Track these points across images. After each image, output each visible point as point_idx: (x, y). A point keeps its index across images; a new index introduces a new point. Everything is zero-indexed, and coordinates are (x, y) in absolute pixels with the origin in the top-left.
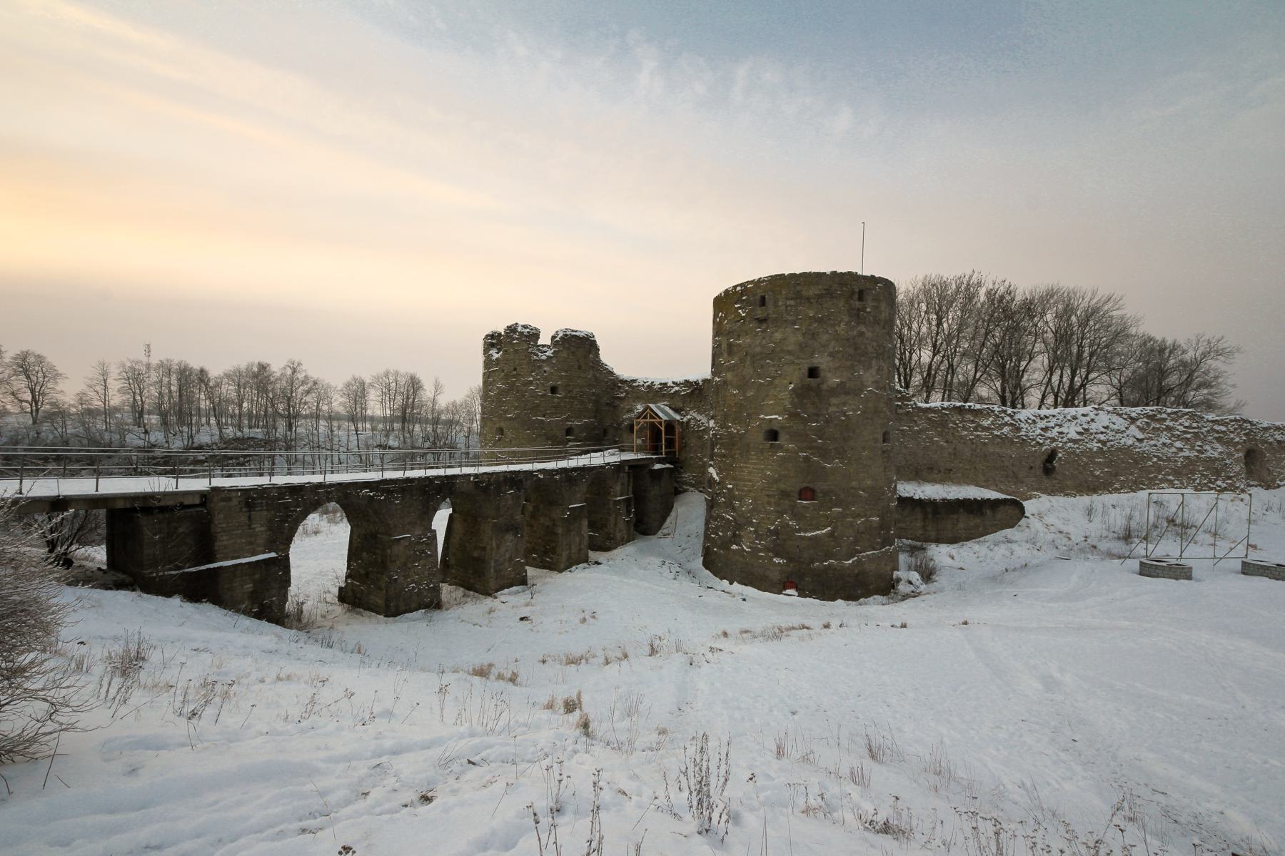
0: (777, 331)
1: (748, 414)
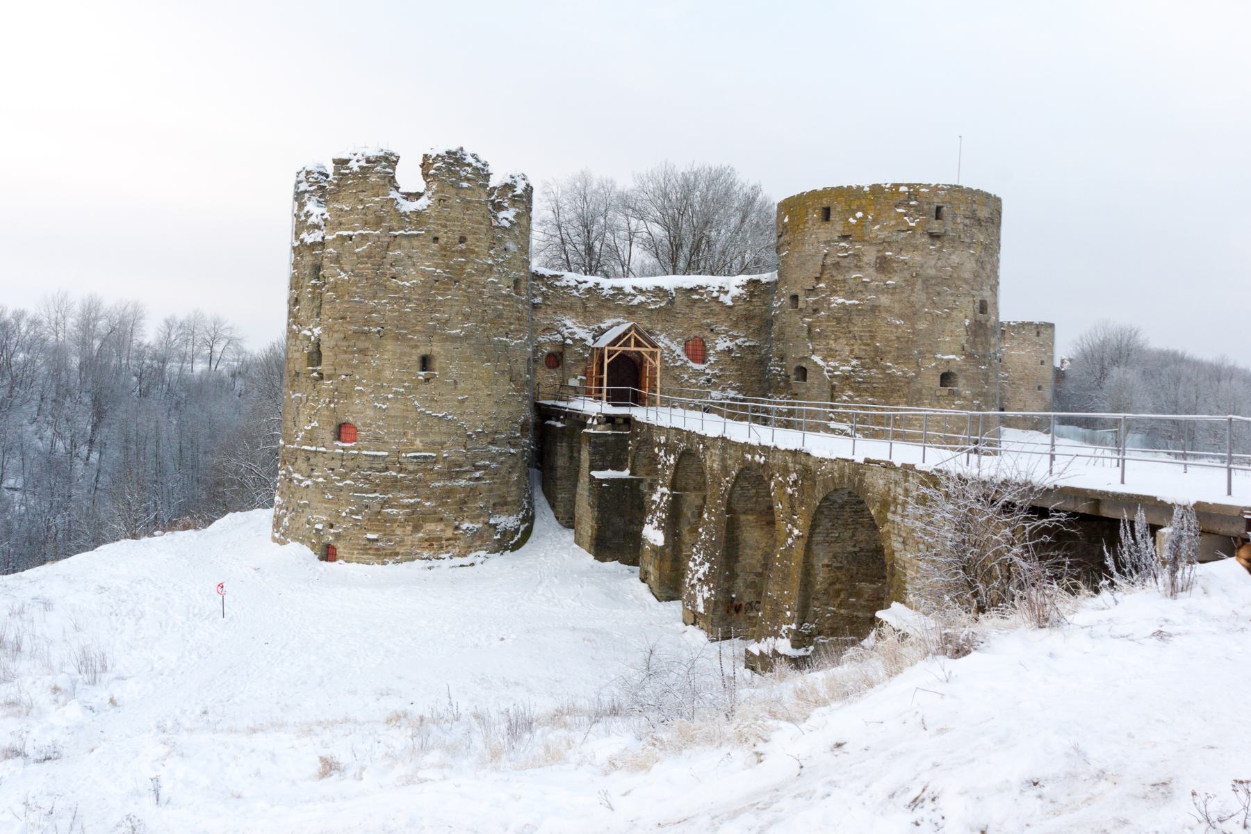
0: (954, 252)
1: (920, 353)
